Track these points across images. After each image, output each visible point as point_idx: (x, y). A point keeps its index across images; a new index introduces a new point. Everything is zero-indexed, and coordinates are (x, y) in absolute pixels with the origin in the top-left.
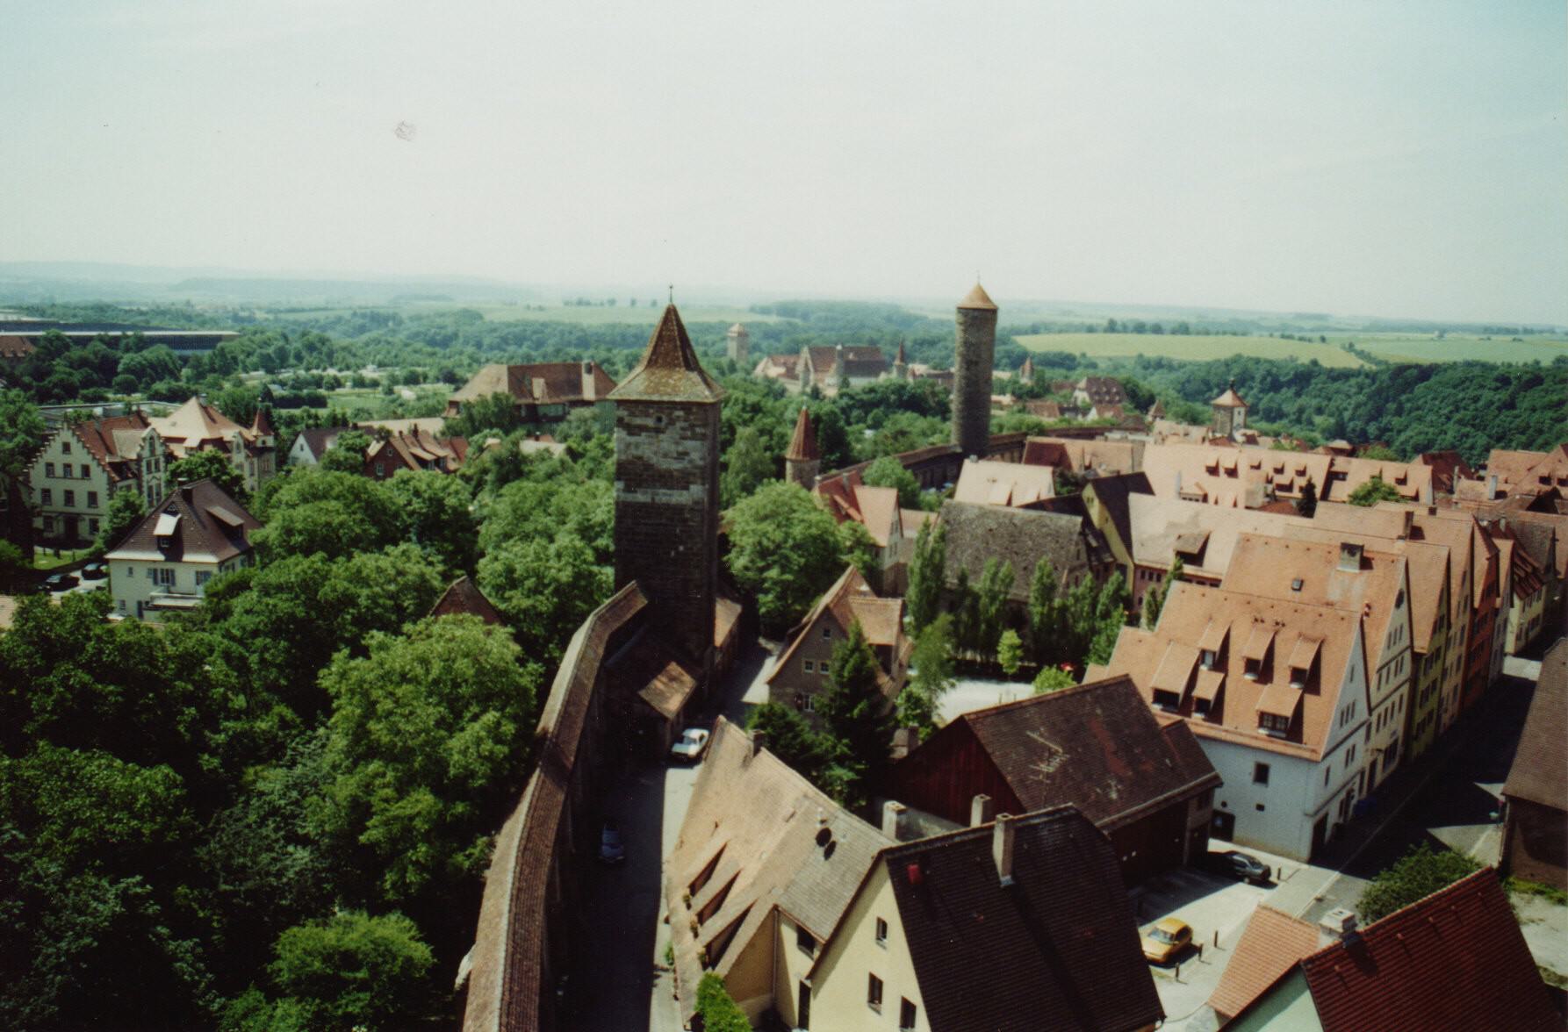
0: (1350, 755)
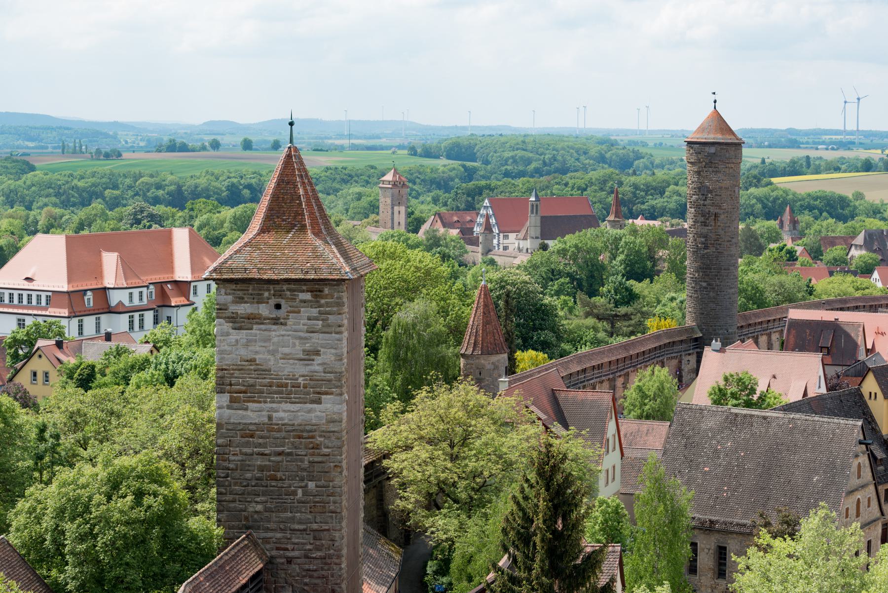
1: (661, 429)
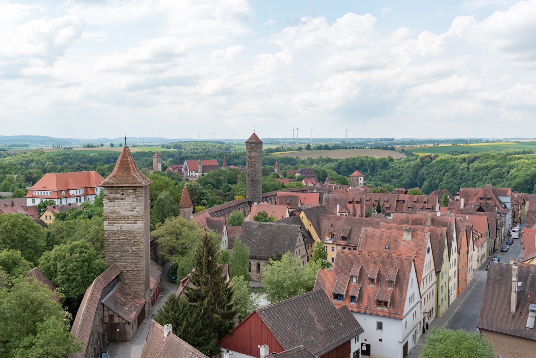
0: (414, 315)
1: (240, 228)
